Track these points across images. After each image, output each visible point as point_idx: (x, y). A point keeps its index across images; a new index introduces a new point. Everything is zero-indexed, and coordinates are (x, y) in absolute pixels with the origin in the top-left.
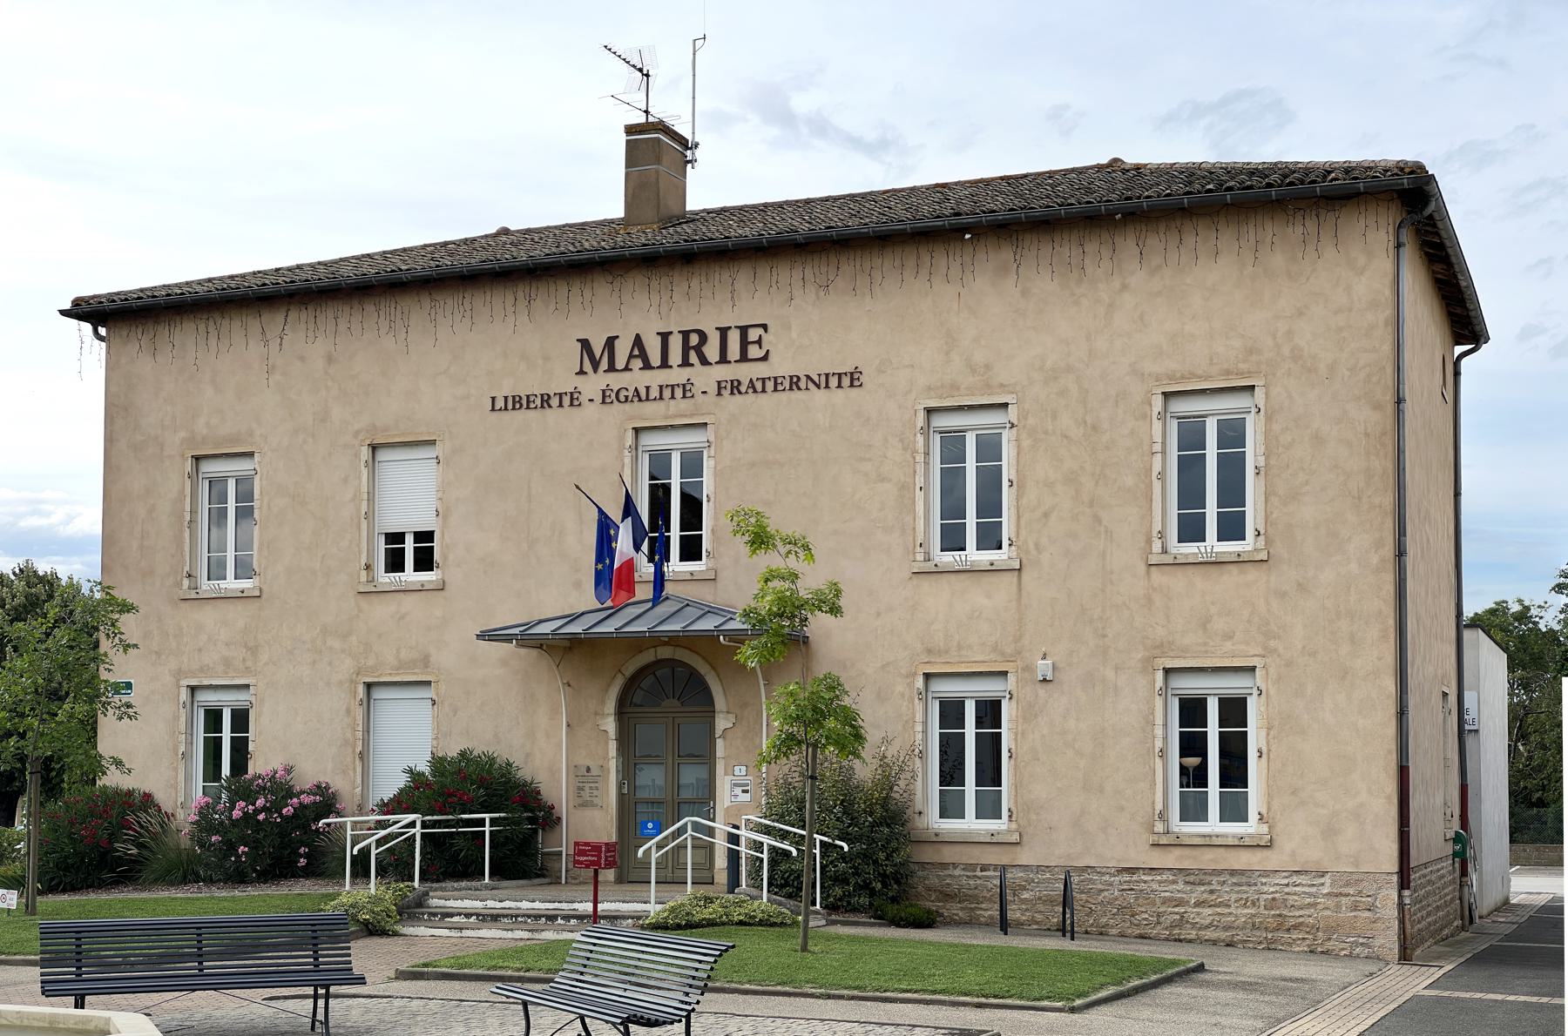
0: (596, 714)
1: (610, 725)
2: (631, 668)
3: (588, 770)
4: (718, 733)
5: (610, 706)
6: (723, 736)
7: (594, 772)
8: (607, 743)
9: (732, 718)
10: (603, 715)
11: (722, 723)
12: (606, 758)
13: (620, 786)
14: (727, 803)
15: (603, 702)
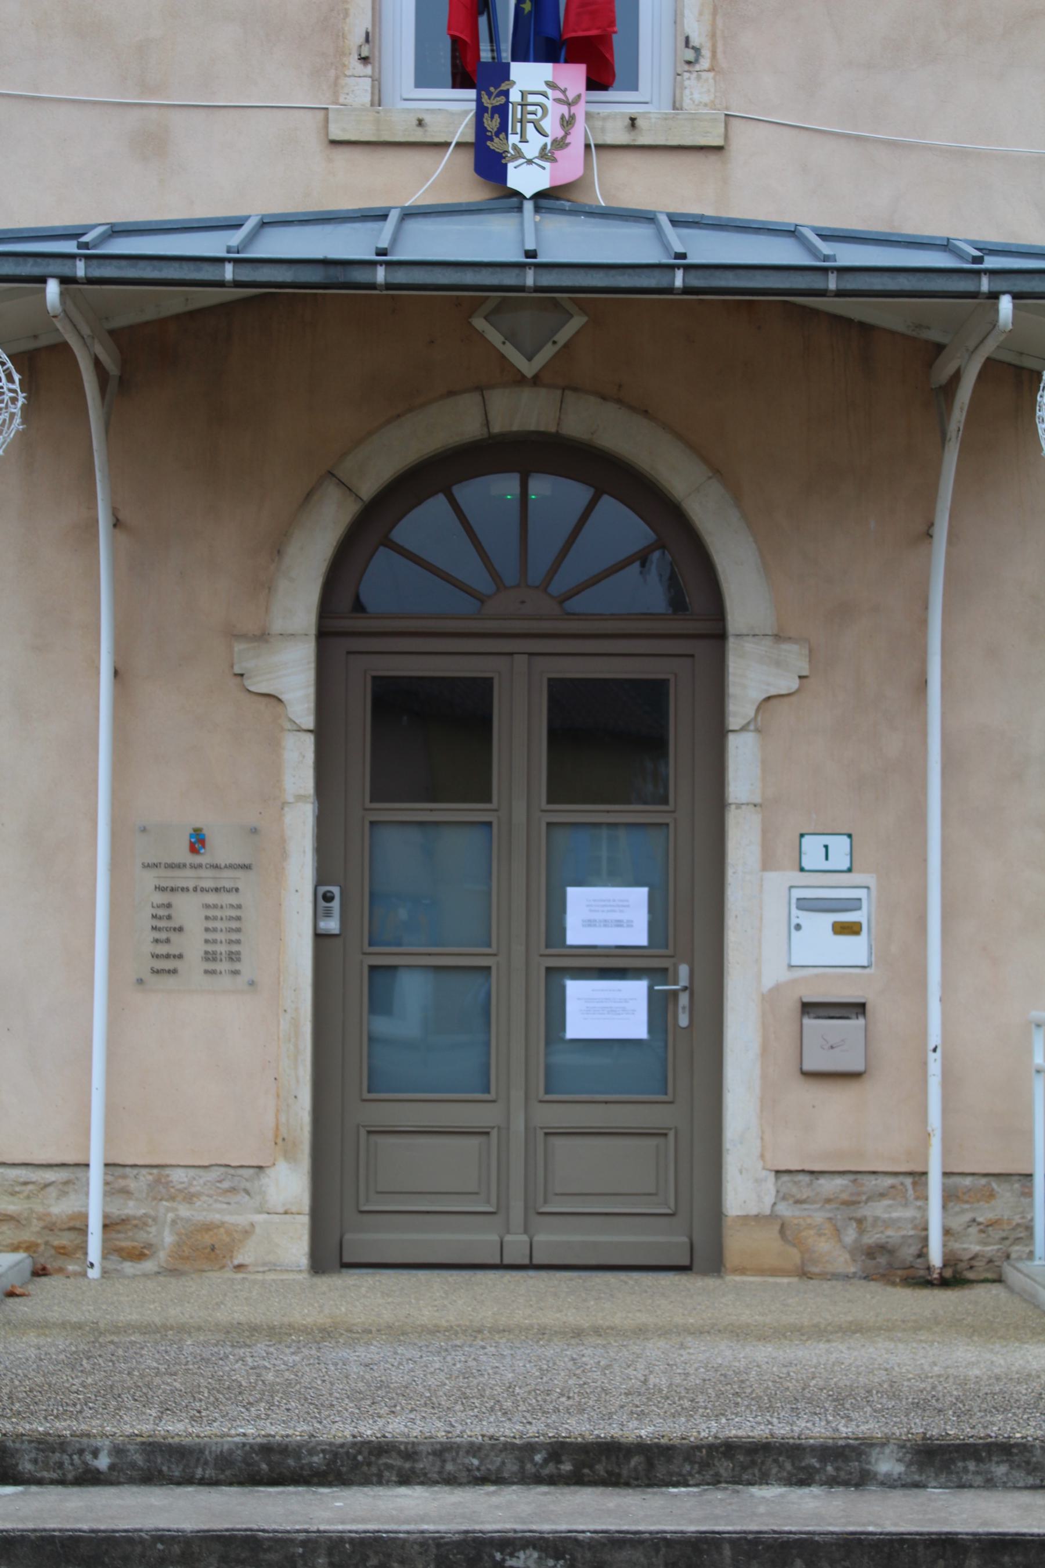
0: (233, 635)
1: (291, 673)
2: (376, 469)
3: (198, 842)
4: (740, 708)
5: (298, 605)
6: (755, 726)
7: (223, 849)
8: (274, 745)
9: (796, 658)
10: (263, 637)
11: (753, 676)
12: (273, 799)
13: (322, 899)
14: (774, 974)
15: (262, 587)
